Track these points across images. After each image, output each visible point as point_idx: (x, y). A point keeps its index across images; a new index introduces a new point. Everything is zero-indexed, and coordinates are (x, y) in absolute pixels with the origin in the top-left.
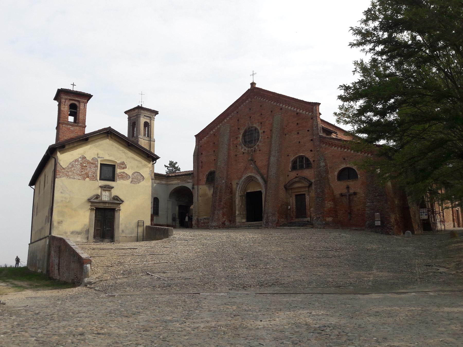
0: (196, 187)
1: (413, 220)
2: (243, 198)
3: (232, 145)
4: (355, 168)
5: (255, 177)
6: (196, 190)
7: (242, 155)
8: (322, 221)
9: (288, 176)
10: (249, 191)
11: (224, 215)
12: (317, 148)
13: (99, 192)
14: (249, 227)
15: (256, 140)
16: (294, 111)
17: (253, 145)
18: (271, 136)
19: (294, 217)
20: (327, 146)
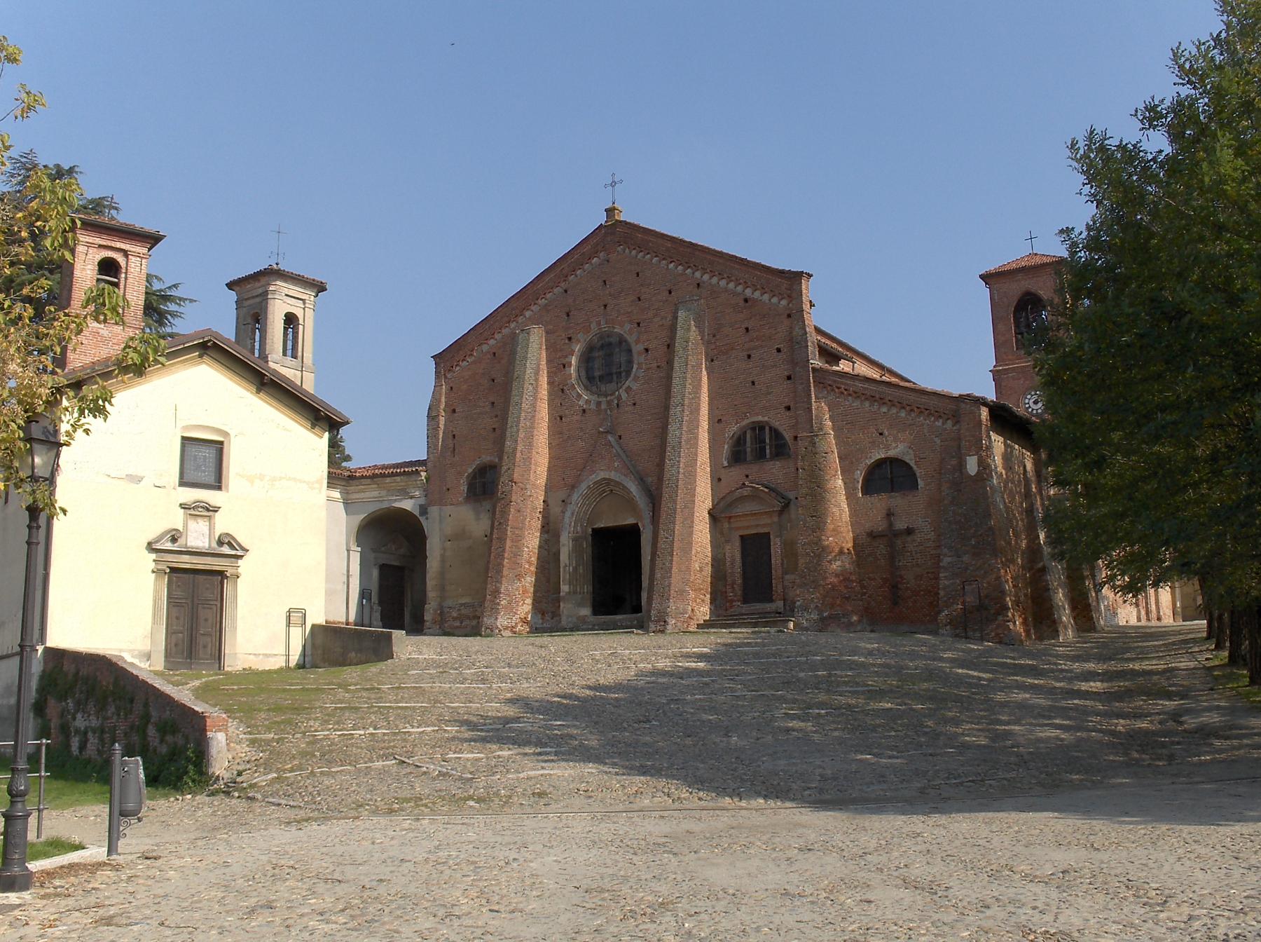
0: (434, 511)
5: (618, 484)
7: (575, 418)
13: (177, 519)
14: (605, 627)
15: (623, 374)
16: (735, 294)
17: (613, 386)
18: (670, 363)
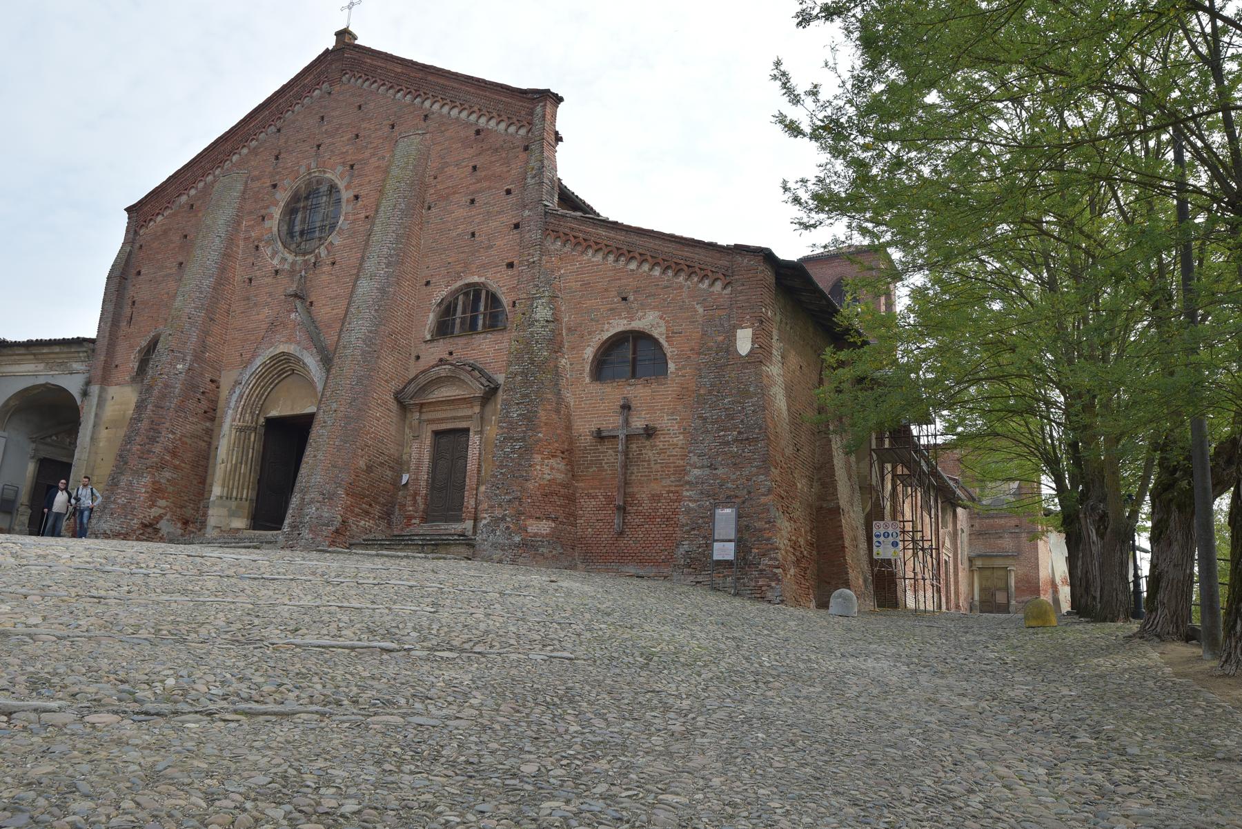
0: (95, 389)
1: (849, 560)
2: (249, 439)
3: (241, 243)
4: (661, 334)
5: (299, 360)
6: (94, 400)
8: (510, 535)
9: (418, 358)
10: (274, 413)
11: (157, 491)
12: (529, 255)
16: (467, 125)
17: (315, 243)
19: (415, 518)
20: (568, 248)
